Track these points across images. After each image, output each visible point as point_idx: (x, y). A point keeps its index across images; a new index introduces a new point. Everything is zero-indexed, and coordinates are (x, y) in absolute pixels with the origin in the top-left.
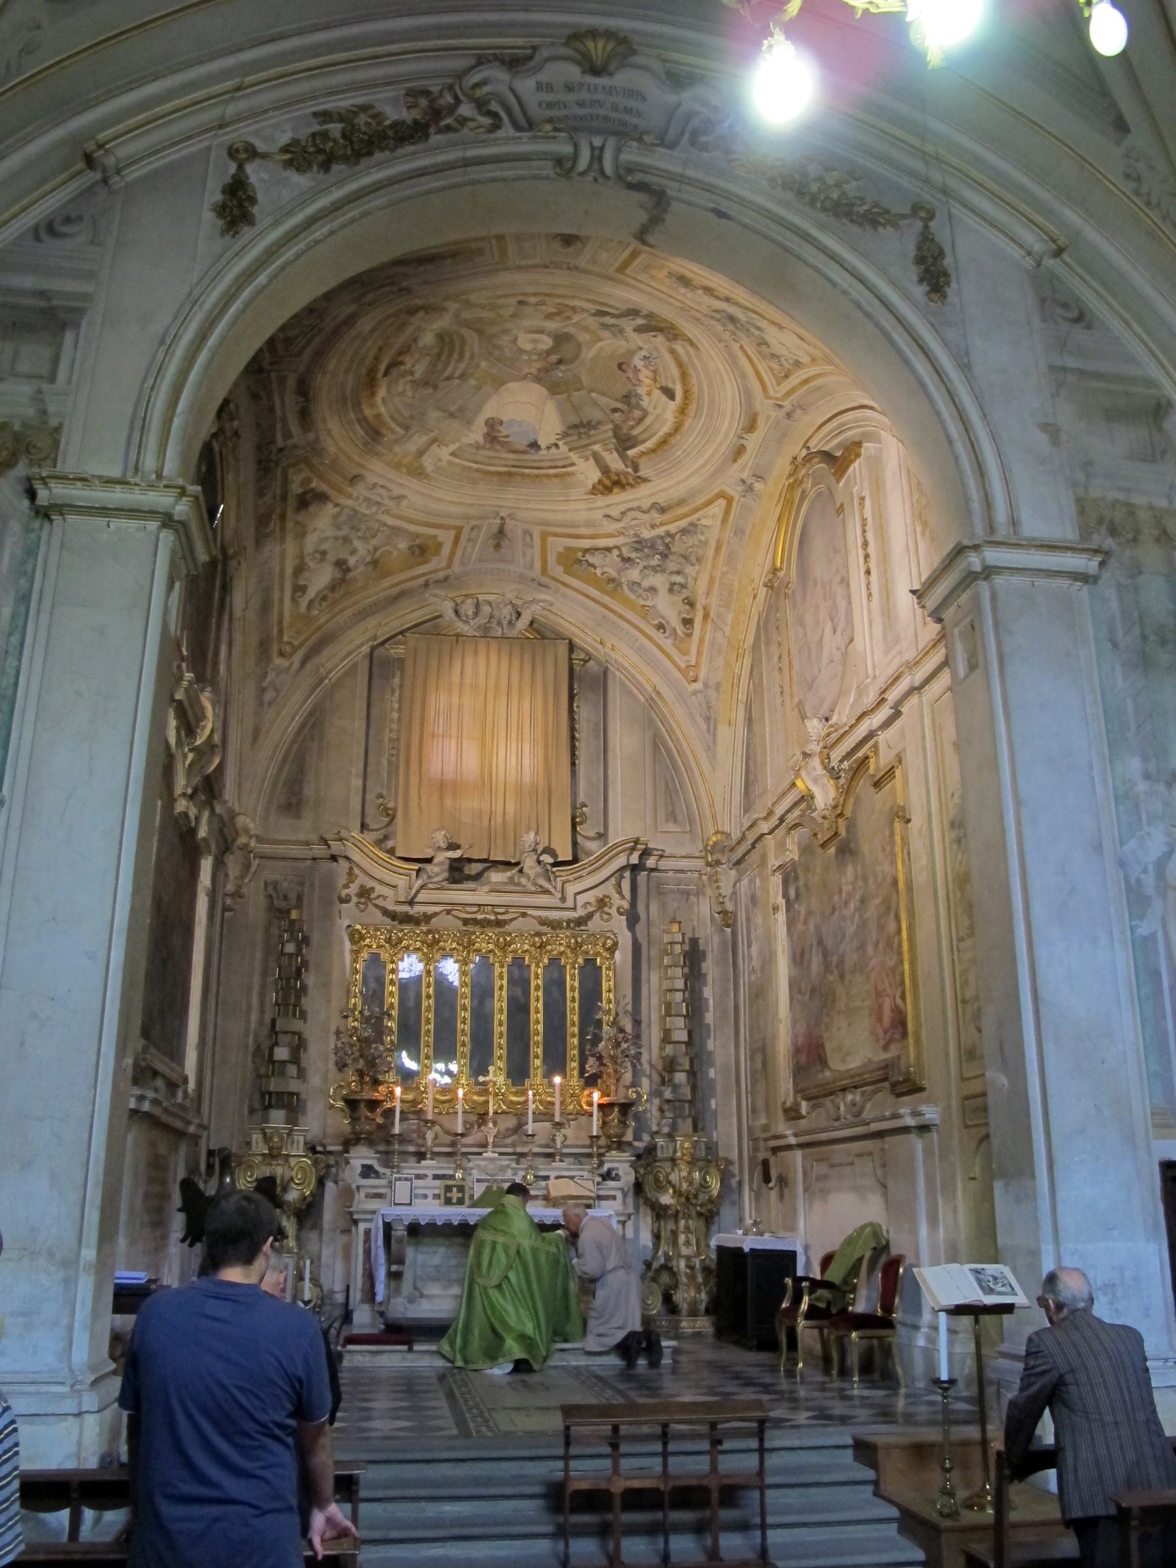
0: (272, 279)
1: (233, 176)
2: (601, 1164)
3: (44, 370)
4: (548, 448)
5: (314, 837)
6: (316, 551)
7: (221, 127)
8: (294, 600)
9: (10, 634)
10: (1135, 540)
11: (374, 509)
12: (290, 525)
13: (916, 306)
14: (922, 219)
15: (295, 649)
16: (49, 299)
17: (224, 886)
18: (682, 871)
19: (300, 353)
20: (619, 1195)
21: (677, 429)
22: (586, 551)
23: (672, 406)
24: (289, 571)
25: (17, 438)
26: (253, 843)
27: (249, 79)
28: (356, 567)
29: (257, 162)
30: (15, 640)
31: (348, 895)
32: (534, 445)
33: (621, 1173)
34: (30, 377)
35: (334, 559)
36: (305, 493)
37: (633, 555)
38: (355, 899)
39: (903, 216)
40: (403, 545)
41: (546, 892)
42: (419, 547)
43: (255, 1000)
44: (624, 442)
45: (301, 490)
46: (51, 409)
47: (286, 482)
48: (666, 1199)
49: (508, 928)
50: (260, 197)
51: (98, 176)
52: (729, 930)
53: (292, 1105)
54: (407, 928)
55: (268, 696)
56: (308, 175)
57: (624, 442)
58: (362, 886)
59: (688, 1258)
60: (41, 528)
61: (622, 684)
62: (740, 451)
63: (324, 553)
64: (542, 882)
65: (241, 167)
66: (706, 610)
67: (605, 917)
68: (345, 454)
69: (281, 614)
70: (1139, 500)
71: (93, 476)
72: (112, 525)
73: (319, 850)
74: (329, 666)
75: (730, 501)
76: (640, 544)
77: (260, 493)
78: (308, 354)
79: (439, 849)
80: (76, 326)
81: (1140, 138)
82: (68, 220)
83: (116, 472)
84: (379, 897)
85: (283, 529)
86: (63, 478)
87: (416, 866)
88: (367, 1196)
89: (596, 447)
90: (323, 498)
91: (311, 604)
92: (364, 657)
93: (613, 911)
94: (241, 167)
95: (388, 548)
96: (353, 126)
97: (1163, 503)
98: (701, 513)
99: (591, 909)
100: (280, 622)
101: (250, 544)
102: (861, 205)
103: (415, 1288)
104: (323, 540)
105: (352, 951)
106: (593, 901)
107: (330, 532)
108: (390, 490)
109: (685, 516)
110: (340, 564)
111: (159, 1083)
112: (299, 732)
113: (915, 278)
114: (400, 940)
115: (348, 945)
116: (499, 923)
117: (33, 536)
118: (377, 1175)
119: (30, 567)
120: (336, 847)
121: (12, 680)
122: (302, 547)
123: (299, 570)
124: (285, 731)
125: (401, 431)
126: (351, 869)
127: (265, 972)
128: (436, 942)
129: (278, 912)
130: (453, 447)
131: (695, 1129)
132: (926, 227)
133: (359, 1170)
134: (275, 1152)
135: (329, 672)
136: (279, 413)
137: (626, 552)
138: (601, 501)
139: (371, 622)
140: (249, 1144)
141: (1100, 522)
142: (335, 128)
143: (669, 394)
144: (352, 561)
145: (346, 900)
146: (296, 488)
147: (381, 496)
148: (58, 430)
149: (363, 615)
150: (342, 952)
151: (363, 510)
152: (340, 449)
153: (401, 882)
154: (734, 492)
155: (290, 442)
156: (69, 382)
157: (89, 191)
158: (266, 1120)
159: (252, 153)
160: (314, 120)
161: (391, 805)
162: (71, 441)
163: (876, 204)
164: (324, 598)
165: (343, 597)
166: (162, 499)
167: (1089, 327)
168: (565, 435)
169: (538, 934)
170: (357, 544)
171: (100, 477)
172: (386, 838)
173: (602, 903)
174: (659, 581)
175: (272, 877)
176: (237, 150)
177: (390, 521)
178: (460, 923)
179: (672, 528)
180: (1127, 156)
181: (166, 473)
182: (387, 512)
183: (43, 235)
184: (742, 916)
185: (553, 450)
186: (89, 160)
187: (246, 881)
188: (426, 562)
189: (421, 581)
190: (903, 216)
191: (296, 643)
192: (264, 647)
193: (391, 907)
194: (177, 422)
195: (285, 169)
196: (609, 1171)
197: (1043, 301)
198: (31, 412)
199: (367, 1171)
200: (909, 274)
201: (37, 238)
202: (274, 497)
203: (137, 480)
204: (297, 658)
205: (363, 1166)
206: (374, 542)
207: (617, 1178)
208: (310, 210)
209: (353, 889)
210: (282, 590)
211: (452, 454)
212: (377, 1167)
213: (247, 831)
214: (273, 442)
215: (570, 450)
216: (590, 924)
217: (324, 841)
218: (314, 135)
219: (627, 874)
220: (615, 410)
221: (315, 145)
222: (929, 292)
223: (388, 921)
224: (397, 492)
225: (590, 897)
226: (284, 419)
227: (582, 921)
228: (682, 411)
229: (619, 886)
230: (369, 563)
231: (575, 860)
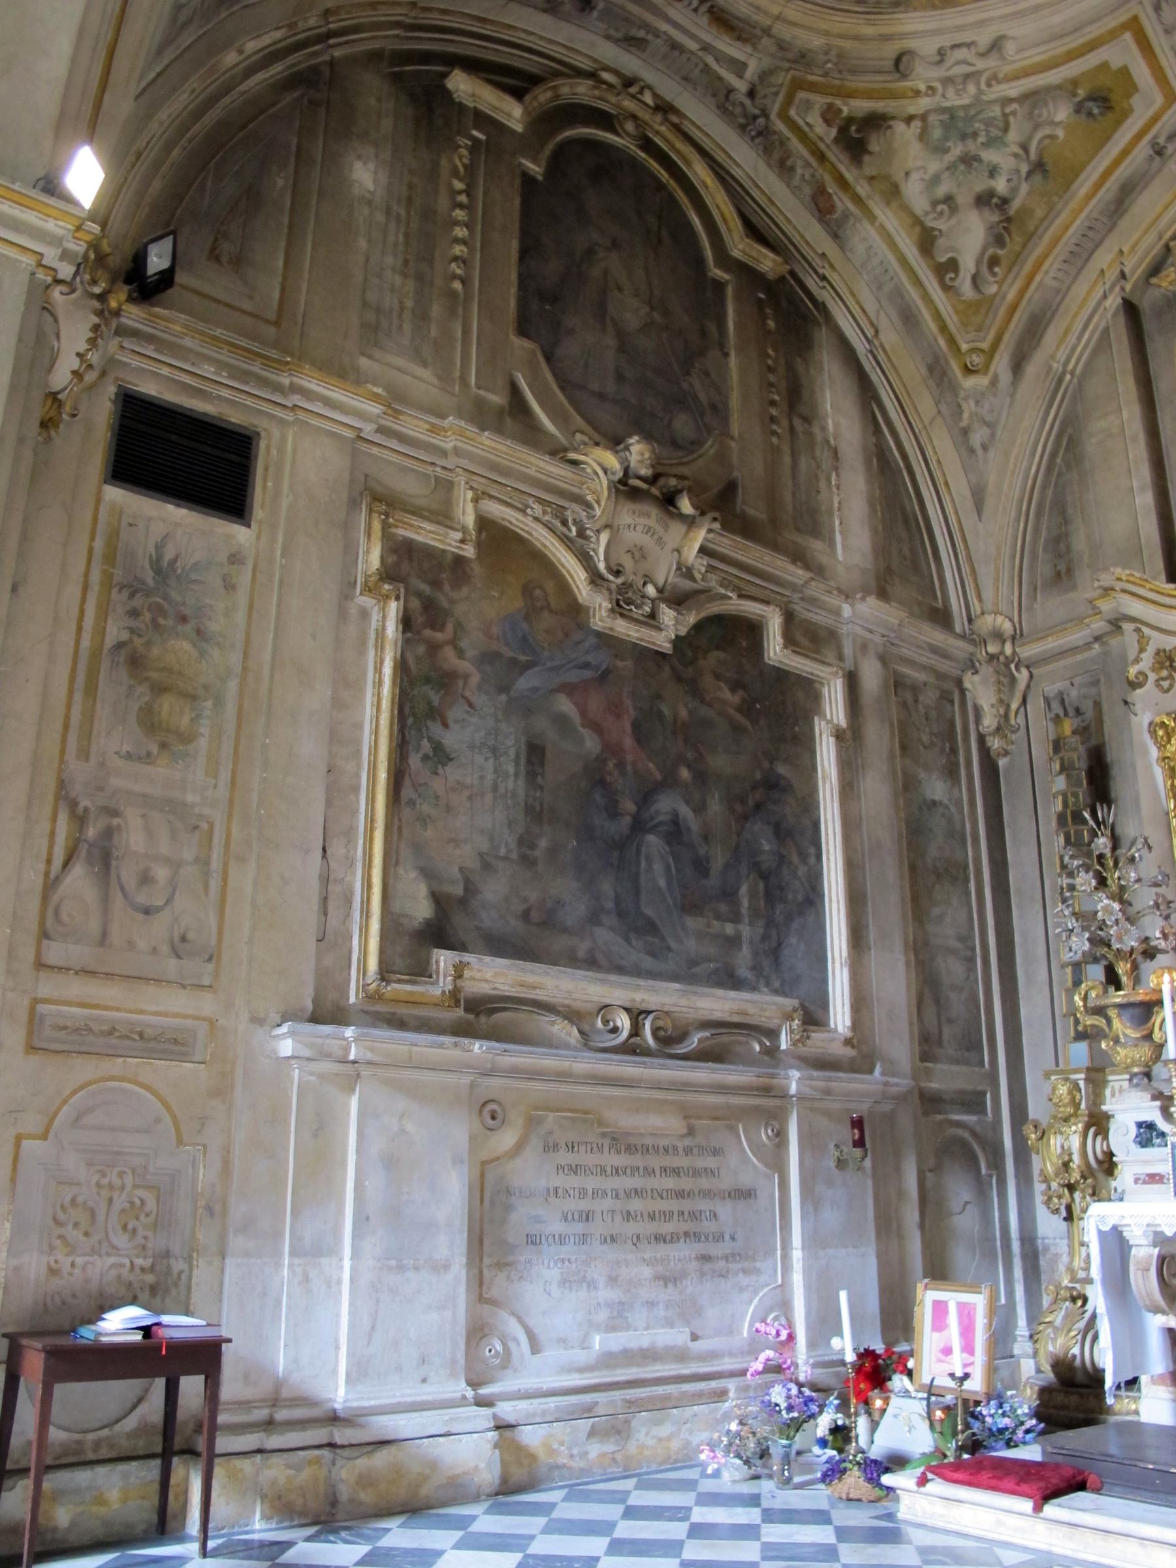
6: (935, 203)
8: (946, 288)
11: (971, 89)
28: (1014, 190)
31: (1141, 673)
35: (971, 199)
36: (843, 130)
38: (1152, 677)
40: (1062, 113)
42: (1091, 98)
45: (834, 132)
55: (978, 437)
58: (1158, 653)
63: (949, 199)
68: (841, 36)
74: (1062, 355)
77: (784, 167)
85: (857, 199)
90: (876, 122)
92: (1115, 315)
95: (1039, 135)
100: (943, 328)
101: (825, 244)
104: (936, 180)
107: (934, 166)
108: (968, 45)
110: (984, 200)
122: (906, 209)
123: (927, 241)
126: (1138, 630)
133: (1133, 1131)
136: (693, 46)
139: (1103, 258)
144: (1001, 186)
146: (825, 133)
147: (964, 62)
149: (1081, 255)
150: (1148, 768)
151: (954, 100)
152: (826, 33)
155: (749, 73)
164: (994, 262)
165: (1024, 246)
170: (991, 156)
175: (1052, 689)
177: (1013, 90)
182: (994, 79)
188: (1126, 113)
189: (1142, 150)
191: (985, 345)
192: (937, 371)
202: (808, 164)
204: (1001, 364)
205: (1140, 1125)
206: (1013, 136)
209: (1147, 658)
210: (918, 283)
213: (998, 636)
214: (730, 91)
224: (984, 39)
226: (706, 48)
230: (1030, 174)
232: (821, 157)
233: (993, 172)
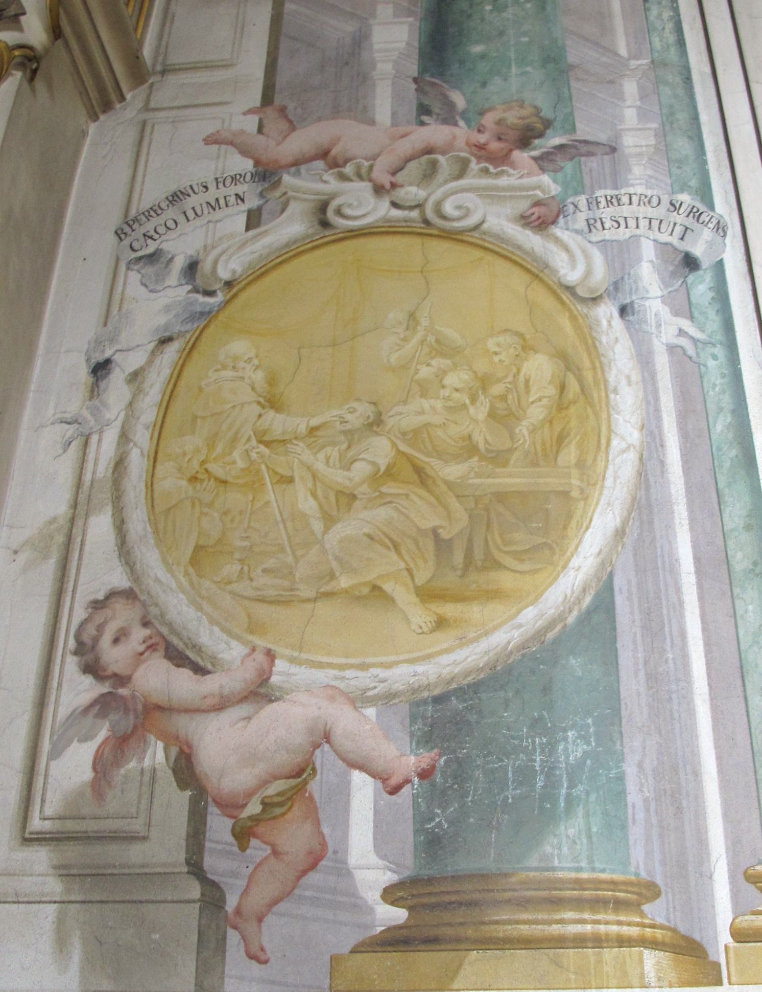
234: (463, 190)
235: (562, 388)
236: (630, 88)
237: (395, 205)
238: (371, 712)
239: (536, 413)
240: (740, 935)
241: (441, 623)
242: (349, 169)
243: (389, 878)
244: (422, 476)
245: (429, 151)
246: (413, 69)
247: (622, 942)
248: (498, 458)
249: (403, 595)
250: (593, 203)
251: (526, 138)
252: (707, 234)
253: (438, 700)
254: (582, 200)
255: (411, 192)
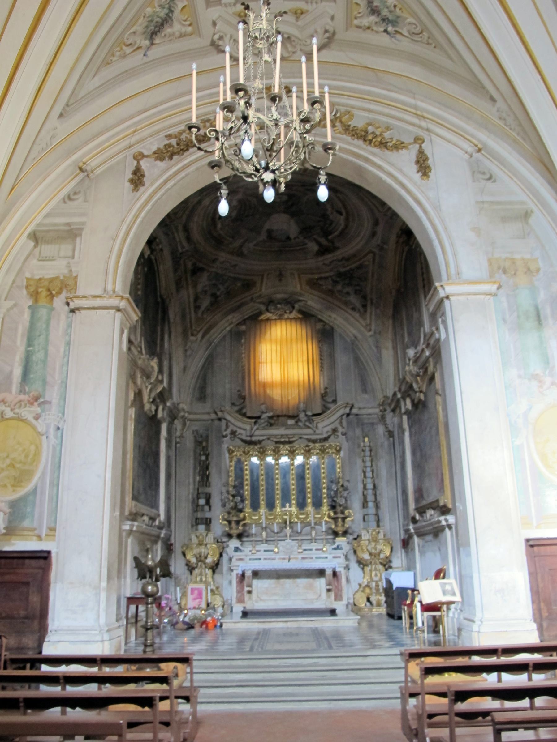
0: (153, 206)
1: (136, 167)
2: (334, 543)
3: (70, 254)
4: (295, 238)
5: (212, 411)
7: (130, 147)
8: (196, 312)
9: (64, 358)
10: (515, 274)
12: (190, 282)
13: (415, 184)
14: (419, 144)
15: (199, 332)
16: (70, 226)
17: (176, 433)
18: (370, 414)
19: (182, 216)
20: (342, 555)
21: (346, 226)
22: (318, 279)
23: (342, 218)
24: (192, 300)
25: (62, 282)
26: (186, 415)
27: (138, 128)
29: (145, 159)
30: (66, 360)
32: (288, 238)
33: (343, 547)
34: (65, 257)
37: (338, 279)
39: (410, 144)
40: (239, 284)
41: (309, 427)
43: (191, 480)
44: (326, 234)
46: (73, 269)
47: (185, 266)
48: (366, 556)
49: (294, 444)
50: (146, 174)
51: (86, 174)
52: (391, 439)
53: (208, 522)
54: (251, 447)
55: (189, 352)
56: (164, 162)
57: (326, 234)
58: (232, 431)
59: (376, 582)
60: (72, 316)
61: (340, 335)
62: (374, 234)
64: (307, 424)
65: (138, 162)
66: (371, 300)
67: (336, 437)
69: (191, 318)
70: (517, 256)
71: (89, 295)
72: (98, 313)
73: (213, 416)
75: (374, 254)
76: (340, 275)
78: (184, 217)
79: (263, 413)
80: (81, 235)
81: (500, 103)
82: (75, 193)
83: (99, 292)
84: (239, 434)
86: (78, 297)
87: (253, 421)
88: (237, 560)
89: (315, 236)
90: (202, 270)
91: (203, 313)
93: (339, 434)
94: (138, 162)
96: (180, 139)
97: (528, 256)
98: (363, 260)
99: (329, 434)
100: (191, 322)
102: (391, 142)
103: (258, 597)
105: (229, 457)
106: (330, 430)
109: (356, 262)
110: (214, 295)
111: (146, 518)
112: (203, 366)
113: (416, 171)
114: (249, 452)
115: (227, 455)
116: (290, 442)
117: (69, 320)
118: (241, 551)
119: (69, 331)
120: (220, 414)
121: (66, 375)
123: (196, 299)
124: (197, 366)
125: (231, 239)
127: (195, 469)
128: (264, 452)
129: (198, 443)
130: (255, 242)
131: (378, 526)
132: (421, 147)
133: (233, 549)
134: (201, 543)
135: (214, 340)
137: (334, 278)
138: (321, 259)
140: (191, 539)
141: (499, 268)
142: (174, 142)
143: (341, 214)
144: (218, 293)
145: (225, 436)
148: (76, 277)
150: (225, 458)
153: (248, 427)
154: (376, 251)
156: (79, 258)
157: (82, 181)
158: (197, 530)
159: (143, 156)
160: (166, 139)
161: (243, 394)
162: (81, 282)
163: (398, 141)
166: (115, 302)
167: (495, 181)
168: (301, 233)
169: (307, 446)
171: (91, 296)
172: (242, 408)
173: (335, 431)
174: (349, 289)
175: (195, 428)
176: (136, 156)
177: (232, 275)
178: (274, 443)
179: (353, 266)
180: (498, 111)
181: (116, 290)
183: (66, 200)
184: (396, 434)
185: (297, 240)
186: (81, 169)
187: (185, 430)
190: (410, 144)
193: (244, 438)
194: (120, 269)
195: (156, 160)
196: (338, 546)
197: (473, 172)
198: (66, 271)
199: (237, 549)
200: (415, 168)
201: (65, 202)
203: (105, 295)
204: (200, 335)
206: (227, 284)
207: (341, 549)
208: (165, 177)
209: (228, 431)
210: (190, 309)
211: (255, 245)
212: (240, 547)
213: (183, 410)
215: (305, 238)
216: (330, 440)
217: (216, 413)
218: (165, 146)
219: (344, 417)
220: (319, 221)
221: (166, 149)
222: (422, 176)
223: (244, 444)
225: (329, 428)
226: (180, 242)
227: (326, 439)
228: (347, 219)
229: (341, 423)
231: (323, 412)
232: (185, 271)
233: (219, 290)
234: (26, 411)
235: (35, 452)
236: (56, 388)
237: (14, 413)
238: (3, 504)
239: (31, 456)
240: (46, 535)
241: (14, 491)
242: (7, 405)
243: (4, 526)
244: (14, 466)
245: (21, 401)
246: (20, 380)
247: (31, 535)
248: (25, 463)
249: (9, 486)
250: (45, 415)
251: (37, 399)
252: (62, 422)
253: (13, 502)
254: (44, 414)
255: (17, 411)
